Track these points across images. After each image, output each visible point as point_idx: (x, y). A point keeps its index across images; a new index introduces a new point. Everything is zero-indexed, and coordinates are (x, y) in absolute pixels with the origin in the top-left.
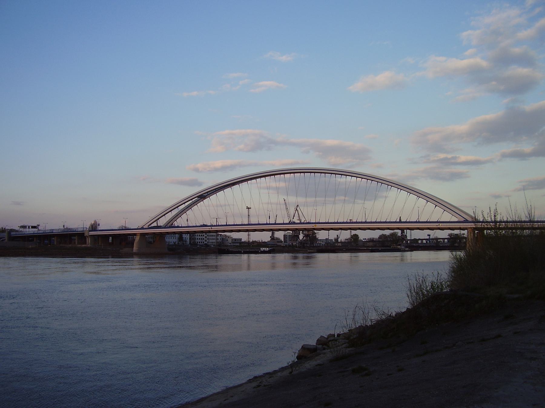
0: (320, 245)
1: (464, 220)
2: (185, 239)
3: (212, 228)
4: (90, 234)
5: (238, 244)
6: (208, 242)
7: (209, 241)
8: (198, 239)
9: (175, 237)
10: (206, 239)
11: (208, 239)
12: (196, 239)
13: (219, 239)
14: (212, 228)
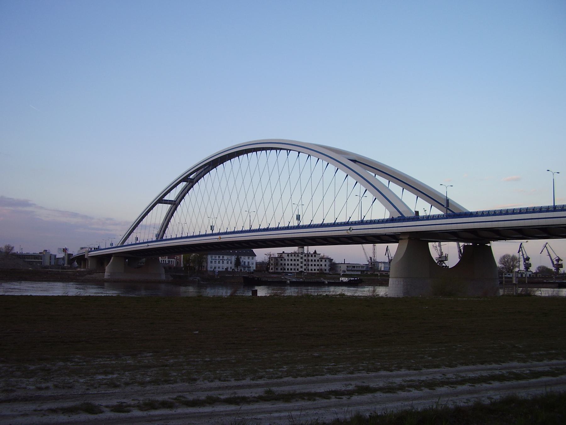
0: (522, 275)
4: (89, 256)
5: (359, 273)
6: (305, 269)
7: (306, 267)
8: (290, 265)
10: (301, 265)
12: (286, 265)
13: (323, 265)
14: (148, 246)
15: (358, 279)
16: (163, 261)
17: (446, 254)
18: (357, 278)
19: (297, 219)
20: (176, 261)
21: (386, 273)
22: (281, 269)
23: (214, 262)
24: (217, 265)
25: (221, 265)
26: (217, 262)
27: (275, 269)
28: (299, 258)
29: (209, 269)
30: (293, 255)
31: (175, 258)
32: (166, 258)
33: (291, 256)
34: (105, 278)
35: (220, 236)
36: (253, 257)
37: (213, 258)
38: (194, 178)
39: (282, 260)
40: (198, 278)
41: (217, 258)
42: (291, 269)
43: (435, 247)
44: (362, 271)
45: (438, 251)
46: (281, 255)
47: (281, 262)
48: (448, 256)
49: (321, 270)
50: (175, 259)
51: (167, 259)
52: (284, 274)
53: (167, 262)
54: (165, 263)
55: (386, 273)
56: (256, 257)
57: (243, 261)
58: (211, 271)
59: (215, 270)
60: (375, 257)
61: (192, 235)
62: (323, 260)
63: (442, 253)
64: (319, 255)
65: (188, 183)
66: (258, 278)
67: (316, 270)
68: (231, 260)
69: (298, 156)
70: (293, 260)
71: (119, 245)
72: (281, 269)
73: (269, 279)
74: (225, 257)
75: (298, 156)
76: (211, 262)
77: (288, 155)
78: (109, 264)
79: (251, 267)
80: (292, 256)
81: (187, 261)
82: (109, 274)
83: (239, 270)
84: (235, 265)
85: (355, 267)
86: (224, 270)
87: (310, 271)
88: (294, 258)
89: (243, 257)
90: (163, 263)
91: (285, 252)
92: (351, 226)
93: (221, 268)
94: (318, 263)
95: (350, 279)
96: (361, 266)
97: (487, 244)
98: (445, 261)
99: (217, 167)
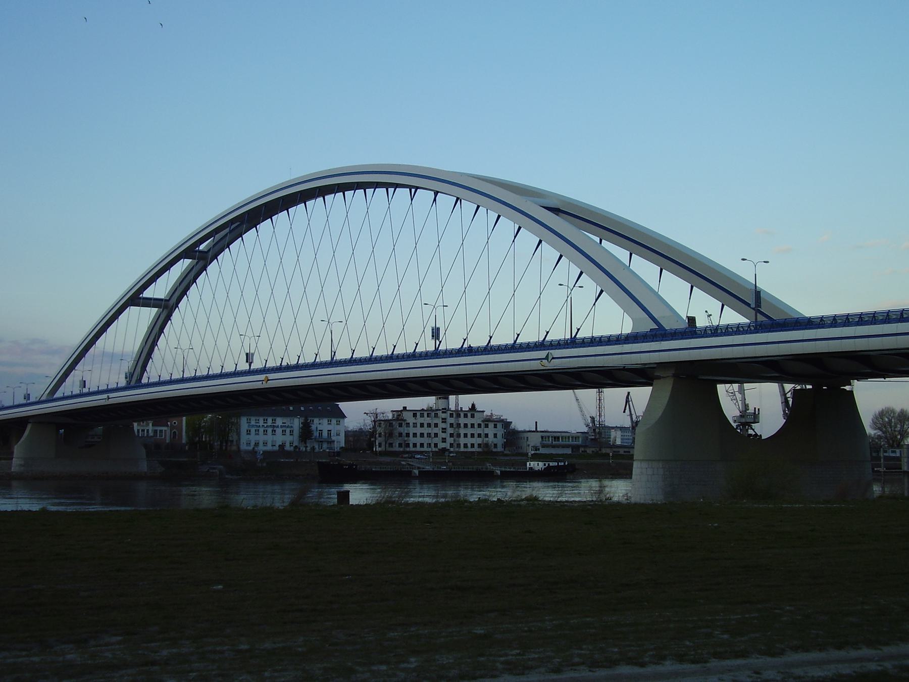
1: (651, 329)
5: (569, 451)
6: (451, 445)
8: (418, 435)
9: (288, 430)
10: (444, 435)
12: (411, 435)
13: (491, 436)
14: (109, 398)
15: (566, 463)
16: (143, 431)
17: (755, 408)
18: (565, 464)
19: (433, 336)
20: (171, 431)
21: (626, 450)
22: (399, 444)
23: (254, 433)
24: (261, 438)
25: (269, 438)
26: (261, 430)
27: (387, 445)
28: (439, 421)
29: (243, 447)
30: (426, 415)
31: (169, 423)
32: (148, 425)
33: (422, 416)
34: (12, 470)
35: (267, 375)
36: (338, 419)
37: (253, 423)
38: (209, 250)
39: (400, 425)
40: (222, 467)
41: (261, 423)
42: (422, 445)
43: (731, 394)
44: (575, 448)
45: (737, 402)
46: (399, 415)
47: (401, 430)
48: (759, 414)
49: (487, 445)
50: (168, 426)
51: (150, 427)
52: (407, 455)
53: (151, 434)
54: (148, 435)
55: (626, 450)
56: (346, 420)
57: (317, 428)
58: (247, 452)
59: (256, 449)
60: (603, 417)
61: (205, 373)
62: (491, 425)
63: (746, 406)
64: (481, 413)
65: (196, 261)
66: (351, 466)
67: (476, 446)
68: (292, 427)
69: (435, 200)
70: (426, 425)
71: (44, 398)
72: (400, 445)
73: (376, 468)
74: (279, 421)
75: (435, 200)
76: (247, 431)
77: (412, 200)
78: (22, 439)
79: (334, 441)
80: (423, 417)
81: (194, 430)
82: (23, 463)
83: (308, 449)
84: (300, 437)
85: (558, 438)
86: (276, 448)
87: (462, 449)
88: (428, 420)
89: (316, 421)
90: (142, 437)
91: (407, 409)
92: (550, 351)
93: (269, 444)
94: (479, 431)
95: (549, 464)
96: (572, 437)
97: (845, 386)
98: (753, 425)
99: (258, 226)
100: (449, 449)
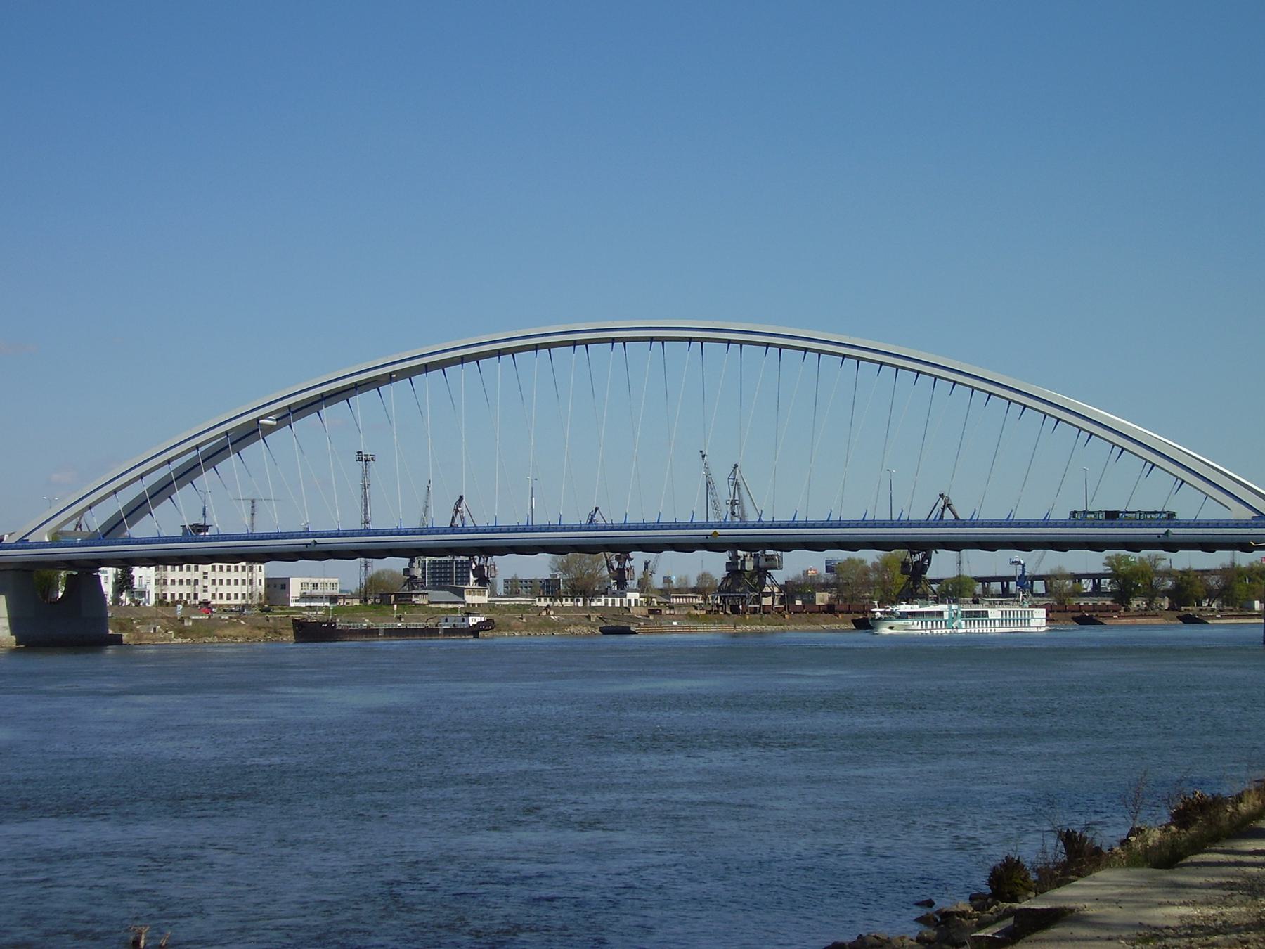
2: (140, 584)
3: (316, 543)
6: (214, 596)
7: (216, 590)
11: (214, 582)
12: (169, 582)
67: (240, 596)
100: (209, 603)
